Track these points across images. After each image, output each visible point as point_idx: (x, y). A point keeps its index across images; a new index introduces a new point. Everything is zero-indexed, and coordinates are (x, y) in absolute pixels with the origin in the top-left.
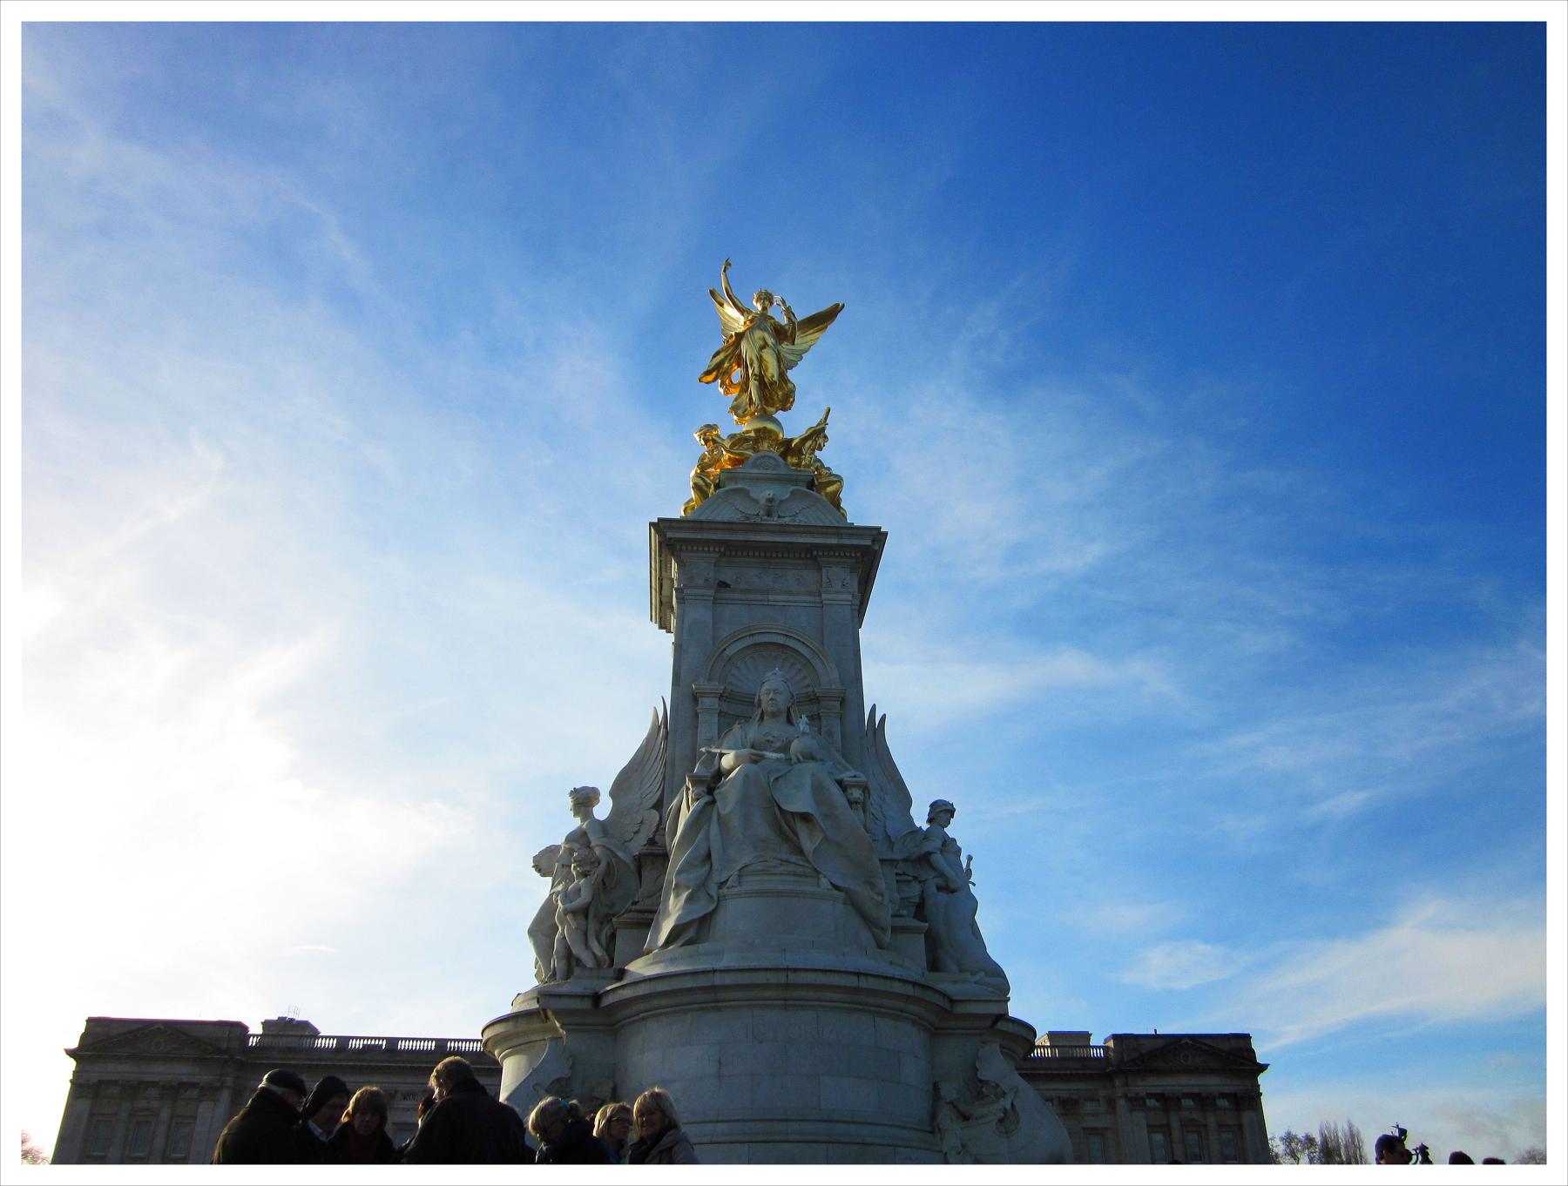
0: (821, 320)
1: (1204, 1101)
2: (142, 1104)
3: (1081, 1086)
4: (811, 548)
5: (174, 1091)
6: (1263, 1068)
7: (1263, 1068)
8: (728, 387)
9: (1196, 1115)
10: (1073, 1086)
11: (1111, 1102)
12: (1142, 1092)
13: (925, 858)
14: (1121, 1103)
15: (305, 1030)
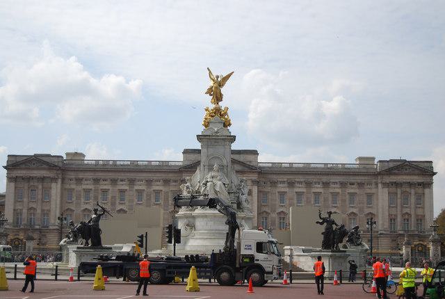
0: (229, 76)
1: (410, 184)
2: (32, 184)
3: (366, 178)
4: (223, 139)
5: (43, 179)
6: (435, 174)
7: (435, 174)
8: (211, 95)
9: (408, 190)
10: (363, 178)
11: (377, 184)
12: (388, 182)
13: (240, 189)
14: (380, 185)
15: (78, 156)
